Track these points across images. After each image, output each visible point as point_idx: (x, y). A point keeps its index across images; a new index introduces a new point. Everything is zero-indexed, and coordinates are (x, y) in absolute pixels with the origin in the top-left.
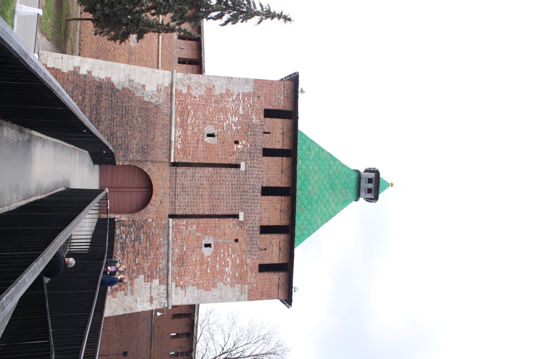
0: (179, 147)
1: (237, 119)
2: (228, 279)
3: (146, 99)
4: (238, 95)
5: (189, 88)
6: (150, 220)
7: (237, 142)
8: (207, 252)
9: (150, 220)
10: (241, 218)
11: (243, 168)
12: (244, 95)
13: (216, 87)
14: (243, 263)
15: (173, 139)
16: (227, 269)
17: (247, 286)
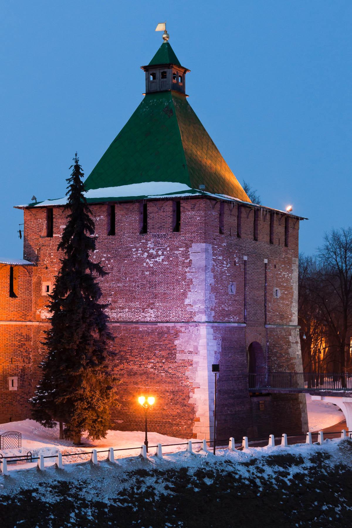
0: (238, 318)
1: (225, 263)
2: (290, 275)
3: (220, 351)
4: (214, 260)
5: (212, 309)
6: (268, 344)
7: (235, 262)
8: (279, 295)
9: (268, 344)
10: (266, 261)
11: (245, 258)
12: (214, 254)
13: (211, 282)
14: (284, 262)
15: (236, 325)
16: (286, 276)
17: (293, 259)
